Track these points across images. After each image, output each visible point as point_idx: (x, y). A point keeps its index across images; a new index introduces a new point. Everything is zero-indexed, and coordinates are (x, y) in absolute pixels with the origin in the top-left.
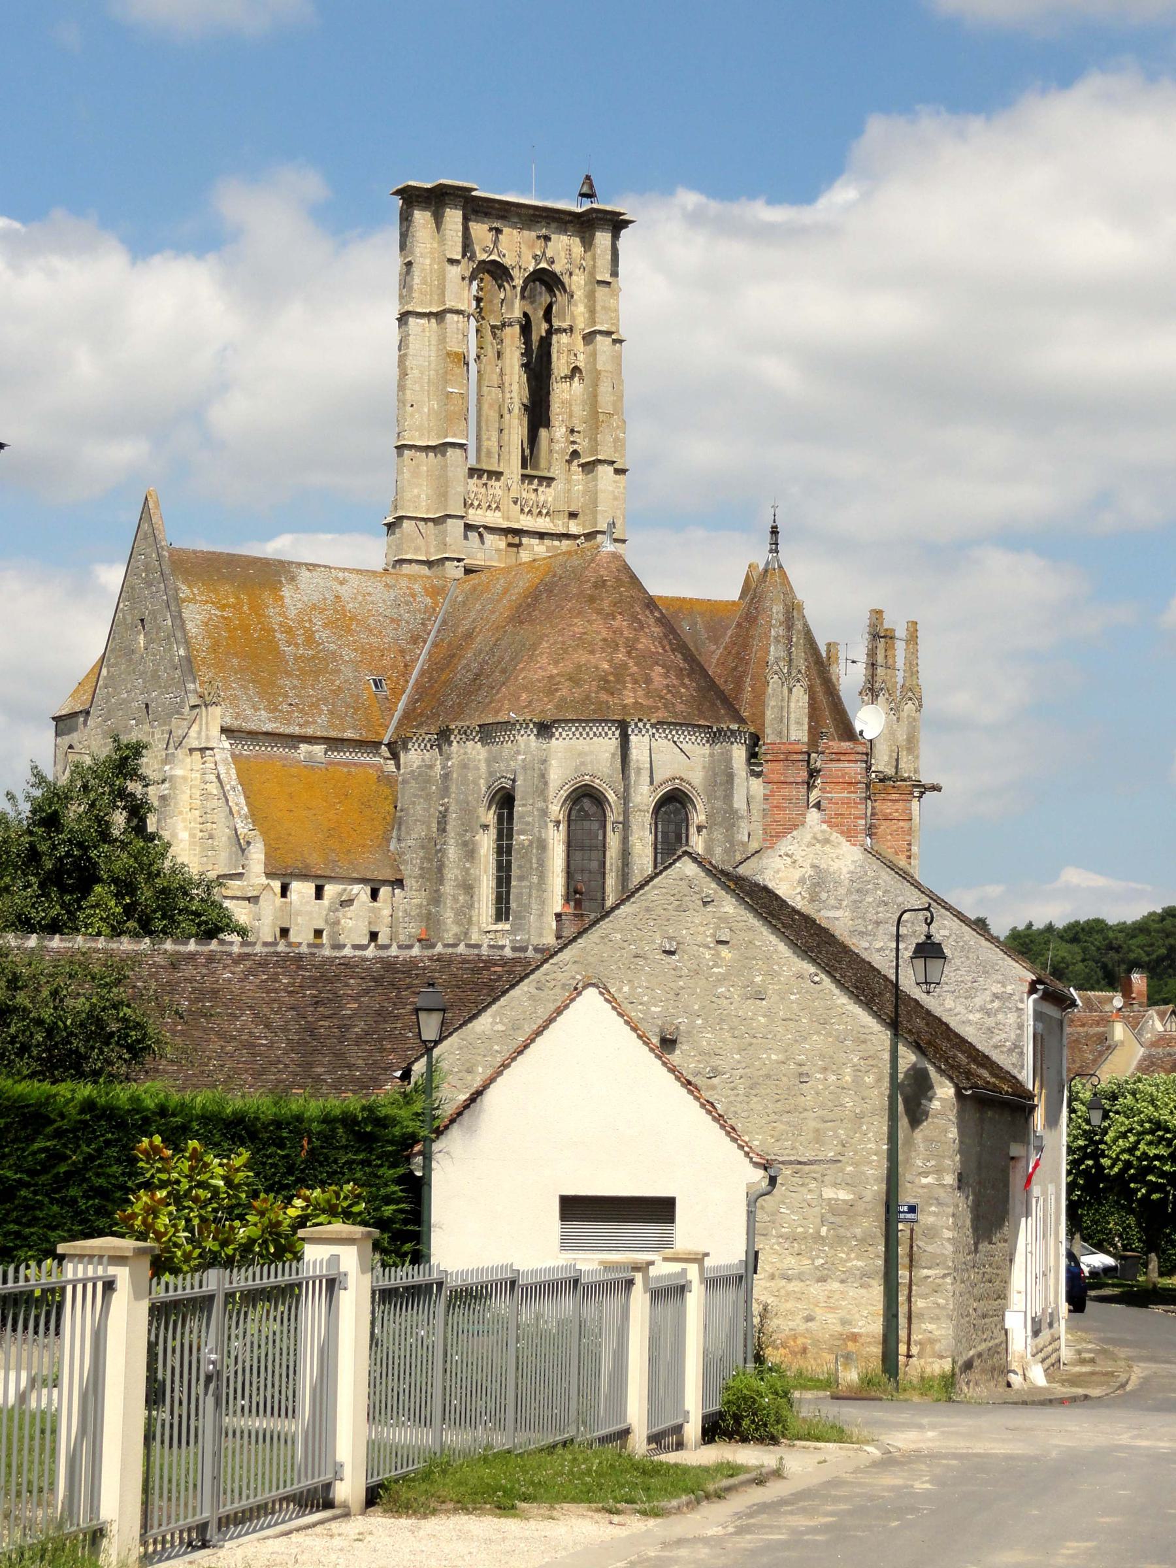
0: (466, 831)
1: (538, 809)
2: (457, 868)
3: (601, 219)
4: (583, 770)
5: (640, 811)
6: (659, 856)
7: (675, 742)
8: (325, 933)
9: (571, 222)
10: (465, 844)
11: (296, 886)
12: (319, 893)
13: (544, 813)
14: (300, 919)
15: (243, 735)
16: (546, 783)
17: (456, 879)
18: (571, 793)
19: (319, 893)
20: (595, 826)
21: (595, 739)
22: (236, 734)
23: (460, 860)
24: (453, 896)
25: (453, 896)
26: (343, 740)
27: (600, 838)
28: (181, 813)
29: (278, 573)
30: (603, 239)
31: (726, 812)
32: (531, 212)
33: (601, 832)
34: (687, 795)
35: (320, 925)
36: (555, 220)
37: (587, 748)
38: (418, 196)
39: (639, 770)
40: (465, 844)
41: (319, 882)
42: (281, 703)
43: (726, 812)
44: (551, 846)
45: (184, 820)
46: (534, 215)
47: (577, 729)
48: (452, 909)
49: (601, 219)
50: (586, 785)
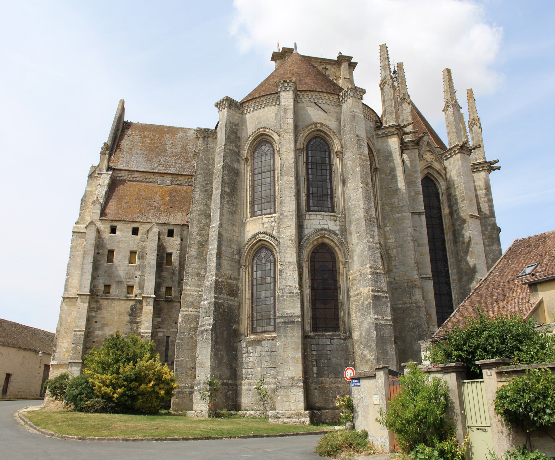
0: (207, 184)
1: (230, 149)
2: (201, 204)
3: (343, 60)
4: (259, 126)
5: (287, 133)
6: (310, 171)
7: (315, 103)
8: (137, 253)
9: (334, 64)
10: (206, 191)
11: (119, 226)
12: (135, 231)
13: (238, 154)
14: (121, 245)
15: (126, 172)
16: (239, 138)
17: (200, 210)
18: (255, 140)
19: (135, 231)
20: (268, 157)
21: (266, 108)
22: (122, 172)
23: (203, 200)
24: (198, 220)
25: (198, 220)
26: (181, 175)
27: (272, 163)
28: (88, 208)
29: (179, 131)
30: (344, 67)
31: (351, 139)
32: (320, 61)
33: (272, 161)
34: (325, 133)
35: (135, 249)
36: (329, 64)
37: (261, 114)
38: (277, 56)
39: (285, 111)
40: (206, 191)
41: (135, 225)
42: (155, 164)
43: (351, 139)
44: (243, 174)
45: (89, 211)
46: (320, 62)
47: (255, 104)
48: (197, 227)
49: (343, 60)
50: (262, 135)
